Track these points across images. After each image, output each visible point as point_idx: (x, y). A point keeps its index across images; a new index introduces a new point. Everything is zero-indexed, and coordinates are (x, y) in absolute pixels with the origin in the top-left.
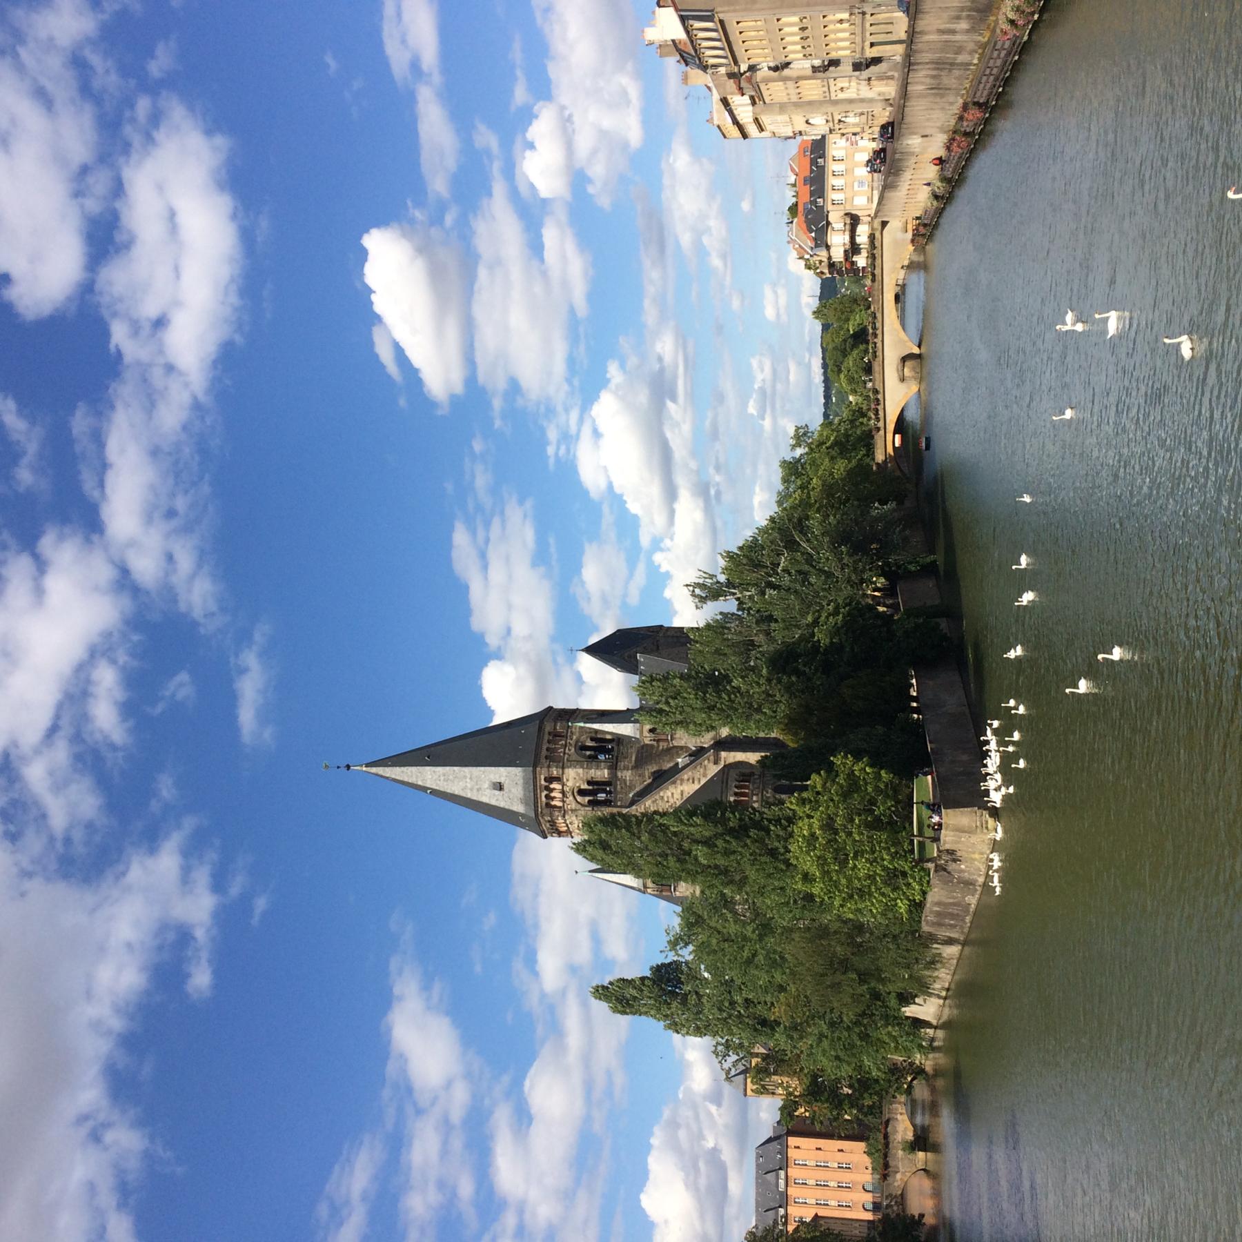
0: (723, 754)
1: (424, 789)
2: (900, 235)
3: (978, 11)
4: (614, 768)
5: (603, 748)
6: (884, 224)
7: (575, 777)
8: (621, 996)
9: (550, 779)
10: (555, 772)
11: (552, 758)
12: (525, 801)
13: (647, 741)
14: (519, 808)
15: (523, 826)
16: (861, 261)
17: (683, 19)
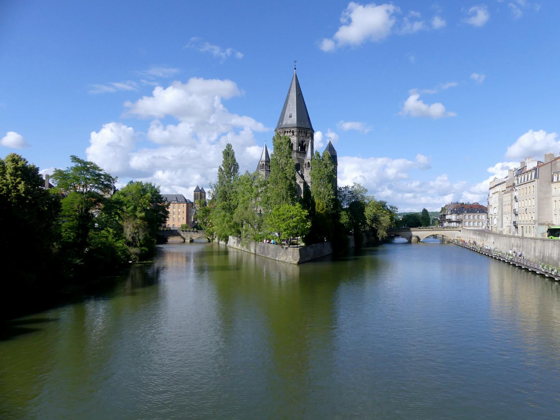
0: (302, 184)
1: (289, 93)
2: (456, 235)
3: (543, 259)
4: (297, 151)
5: (303, 148)
6: (460, 231)
7: (294, 140)
8: (228, 154)
9: (293, 132)
10: (295, 133)
11: (299, 132)
12: (286, 124)
13: (305, 161)
14: (284, 123)
15: (278, 124)
16: (446, 224)
17: (535, 169)
